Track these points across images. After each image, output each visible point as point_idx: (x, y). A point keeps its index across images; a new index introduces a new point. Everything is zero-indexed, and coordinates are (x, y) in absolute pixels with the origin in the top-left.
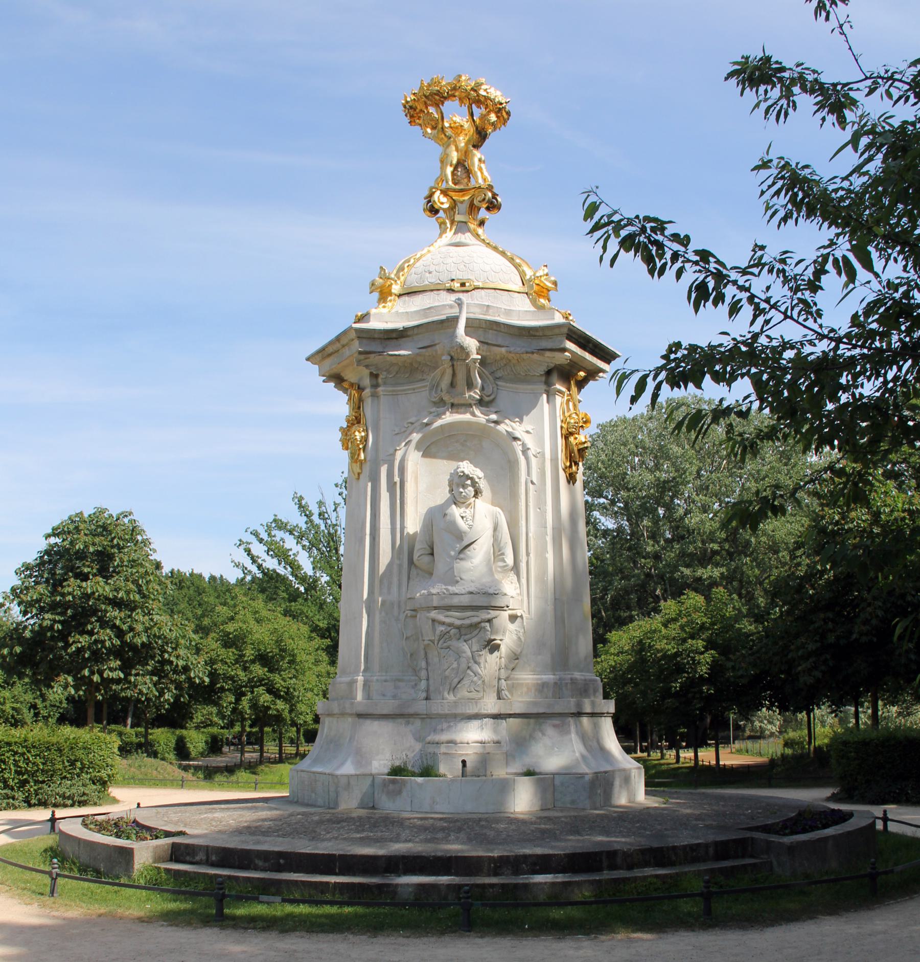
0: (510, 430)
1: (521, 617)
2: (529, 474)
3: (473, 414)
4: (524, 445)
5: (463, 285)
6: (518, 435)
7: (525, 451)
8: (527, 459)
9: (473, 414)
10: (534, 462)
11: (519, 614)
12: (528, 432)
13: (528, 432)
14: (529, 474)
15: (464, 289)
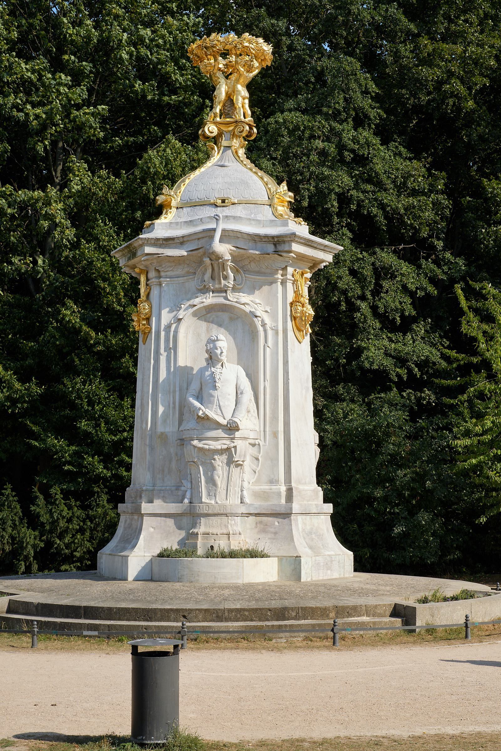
0: (253, 310)
1: (259, 444)
2: (266, 341)
3: (226, 298)
4: (263, 321)
5: (223, 201)
6: (258, 314)
7: (264, 325)
8: (265, 331)
9: (226, 298)
10: (270, 333)
11: (257, 443)
12: (266, 311)
13: (266, 311)
14: (266, 341)
15: (223, 204)
